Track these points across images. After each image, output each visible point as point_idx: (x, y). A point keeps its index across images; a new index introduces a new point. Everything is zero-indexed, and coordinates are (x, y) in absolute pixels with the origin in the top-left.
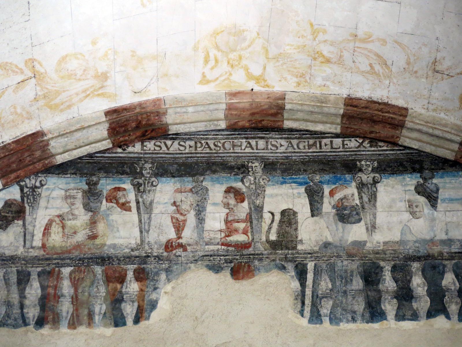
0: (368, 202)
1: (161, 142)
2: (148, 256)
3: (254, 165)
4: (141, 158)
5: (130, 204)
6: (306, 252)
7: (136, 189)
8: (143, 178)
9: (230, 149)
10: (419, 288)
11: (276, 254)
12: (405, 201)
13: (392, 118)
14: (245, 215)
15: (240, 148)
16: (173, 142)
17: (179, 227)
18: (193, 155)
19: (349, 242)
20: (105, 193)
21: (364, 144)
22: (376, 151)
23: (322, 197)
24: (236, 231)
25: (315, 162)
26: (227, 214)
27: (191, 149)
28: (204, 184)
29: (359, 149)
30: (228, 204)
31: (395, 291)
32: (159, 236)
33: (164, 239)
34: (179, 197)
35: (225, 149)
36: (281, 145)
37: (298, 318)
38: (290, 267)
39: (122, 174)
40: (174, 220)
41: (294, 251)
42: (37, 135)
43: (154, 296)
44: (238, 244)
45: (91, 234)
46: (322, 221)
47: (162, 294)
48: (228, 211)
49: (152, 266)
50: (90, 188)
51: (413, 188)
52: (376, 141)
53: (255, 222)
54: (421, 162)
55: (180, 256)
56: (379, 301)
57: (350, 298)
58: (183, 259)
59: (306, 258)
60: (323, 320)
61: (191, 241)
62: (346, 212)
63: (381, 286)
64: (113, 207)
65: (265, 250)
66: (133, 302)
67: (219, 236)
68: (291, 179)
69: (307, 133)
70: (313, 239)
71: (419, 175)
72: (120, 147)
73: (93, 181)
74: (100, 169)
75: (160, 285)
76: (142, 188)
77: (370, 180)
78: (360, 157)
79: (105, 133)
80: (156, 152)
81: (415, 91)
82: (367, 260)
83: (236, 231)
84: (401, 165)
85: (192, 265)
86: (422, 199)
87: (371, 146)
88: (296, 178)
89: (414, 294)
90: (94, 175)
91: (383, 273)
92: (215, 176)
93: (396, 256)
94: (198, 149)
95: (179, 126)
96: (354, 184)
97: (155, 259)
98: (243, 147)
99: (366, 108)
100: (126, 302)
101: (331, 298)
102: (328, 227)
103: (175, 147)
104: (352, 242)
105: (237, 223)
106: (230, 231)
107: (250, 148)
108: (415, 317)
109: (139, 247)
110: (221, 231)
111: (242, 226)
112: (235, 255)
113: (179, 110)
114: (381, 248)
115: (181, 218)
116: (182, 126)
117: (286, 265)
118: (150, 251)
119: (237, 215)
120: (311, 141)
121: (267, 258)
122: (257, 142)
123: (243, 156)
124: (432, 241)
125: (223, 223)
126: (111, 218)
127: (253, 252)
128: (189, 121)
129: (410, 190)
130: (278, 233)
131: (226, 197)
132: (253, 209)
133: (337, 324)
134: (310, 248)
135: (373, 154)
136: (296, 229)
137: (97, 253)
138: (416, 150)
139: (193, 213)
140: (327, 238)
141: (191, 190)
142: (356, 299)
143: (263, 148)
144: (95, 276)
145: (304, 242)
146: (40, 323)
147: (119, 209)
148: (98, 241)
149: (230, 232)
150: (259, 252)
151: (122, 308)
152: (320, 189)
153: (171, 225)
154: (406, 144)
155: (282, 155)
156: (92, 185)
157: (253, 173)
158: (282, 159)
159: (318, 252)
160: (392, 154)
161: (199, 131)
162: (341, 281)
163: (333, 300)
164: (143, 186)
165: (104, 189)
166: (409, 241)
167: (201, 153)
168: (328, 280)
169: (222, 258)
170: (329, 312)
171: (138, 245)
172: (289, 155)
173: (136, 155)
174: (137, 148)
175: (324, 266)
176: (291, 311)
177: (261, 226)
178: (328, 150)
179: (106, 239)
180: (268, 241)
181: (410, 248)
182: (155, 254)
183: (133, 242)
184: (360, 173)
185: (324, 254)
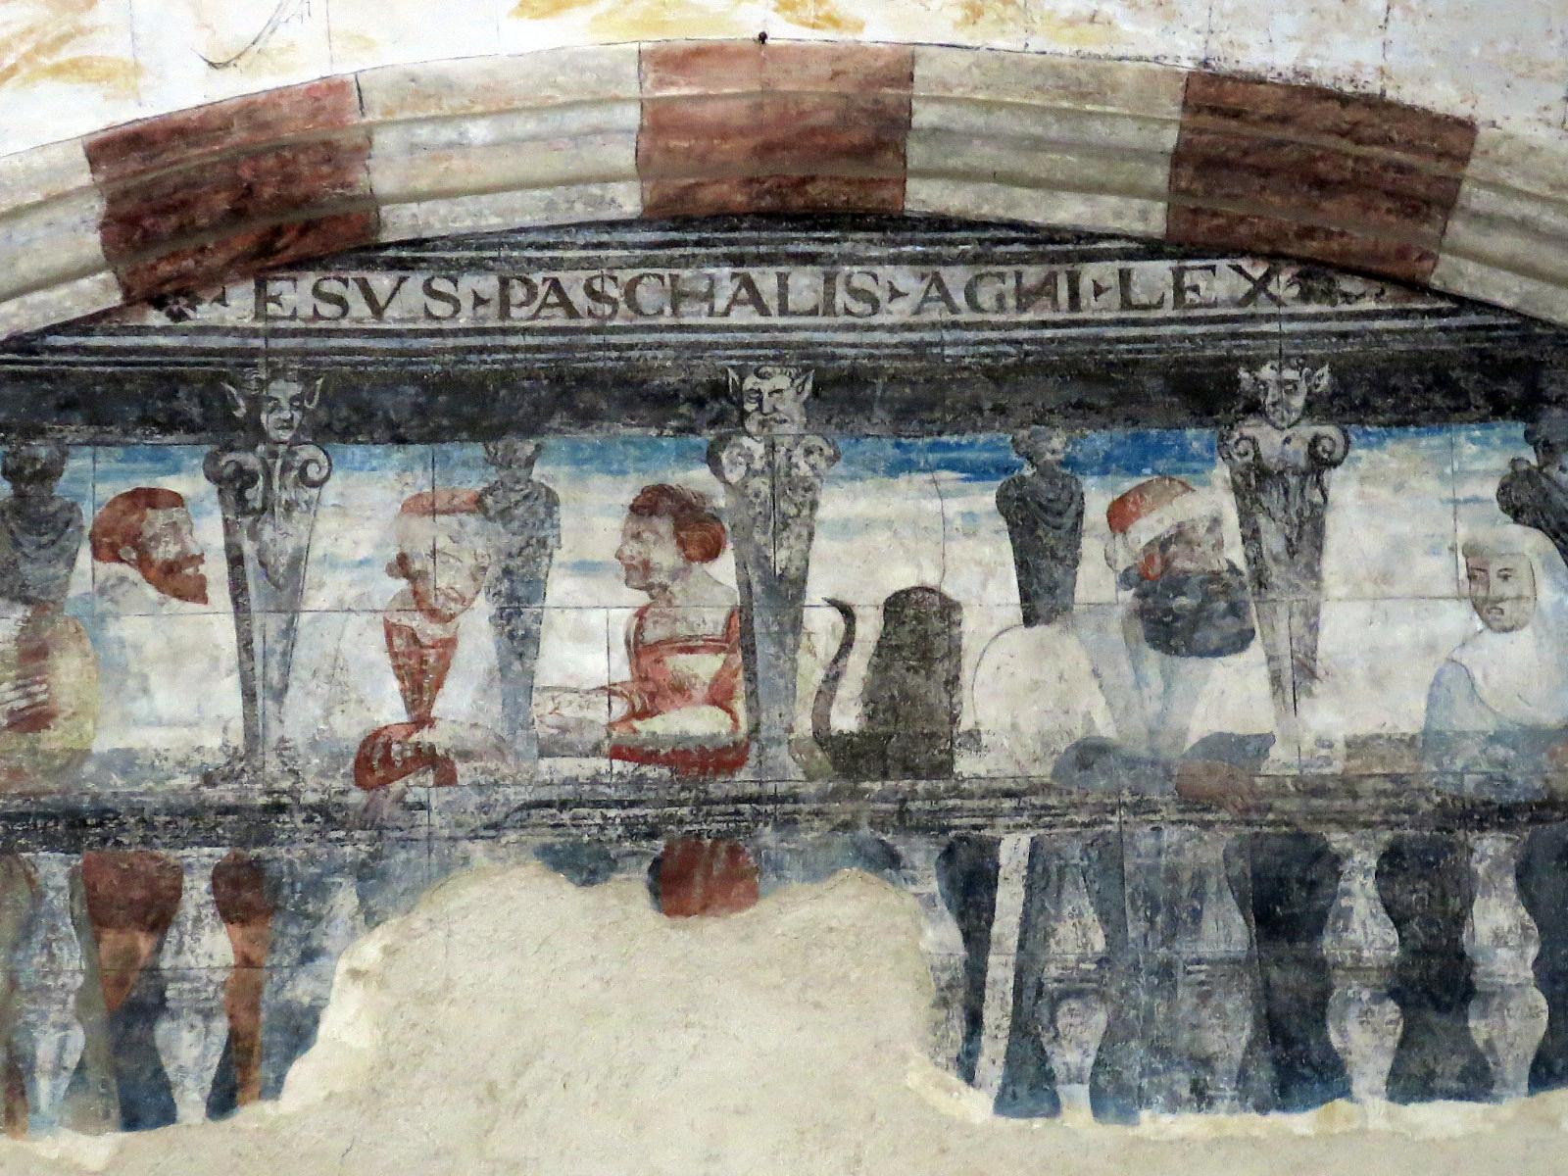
0: (1284, 557)
1: (345, 282)
2: (280, 808)
3: (766, 386)
4: (254, 352)
5: (202, 569)
6: (995, 785)
7: (231, 498)
8: (261, 448)
9: (661, 312)
10: (1502, 953)
11: (856, 795)
12: (1453, 549)
13: (1400, 169)
14: (721, 617)
15: (706, 307)
16: (402, 280)
18: (488, 341)
19: (1193, 739)
20: (88, 515)
21: (1272, 288)
22: (1325, 317)
23: (1076, 530)
24: (681, 689)
25: (1045, 368)
26: (641, 615)
27: (481, 310)
28: (538, 472)
29: (1250, 309)
30: (646, 567)
31: (1390, 967)
32: (328, 713)
33: (349, 729)
34: (424, 533)
35: (639, 312)
36: (895, 294)
37: (949, 1090)
38: (918, 859)
39: (167, 428)
40: (397, 642)
41: (942, 785)
43: (301, 990)
44: (686, 752)
45: (23, 703)
46: (1071, 642)
47: (337, 979)
48: (641, 598)
49: (298, 853)
50: (20, 495)
51: (1490, 490)
52: (1330, 273)
53: (765, 649)
54: (1529, 371)
55: (422, 806)
56: (1317, 1010)
57: (1186, 997)
58: (436, 820)
59: (992, 815)
60: (1063, 1099)
61: (474, 739)
62: (1183, 601)
63: (1328, 945)
64: (122, 579)
65: (810, 778)
66: (208, 1015)
67: (599, 714)
68: (934, 447)
69: (1013, 234)
70: (1029, 725)
71: (1518, 429)
72: (159, 303)
73: (35, 459)
74: (67, 406)
75: (332, 937)
76: (256, 495)
77: (1297, 454)
78: (1252, 348)
79: (91, 244)
80: (322, 324)
81: (1504, 46)
82: (1271, 824)
83: (681, 689)
84: (1442, 381)
85: (478, 850)
87: (1305, 296)
88: (959, 446)
89: (1479, 977)
90: (42, 432)
91: (1342, 884)
92: (591, 437)
93: (1403, 802)
94: (514, 312)
95: (424, 206)
96: (1221, 472)
97: (309, 820)
98: (721, 304)
99: (1284, 120)
100: (174, 1016)
101: (1103, 998)
102: (1096, 673)
104: (1204, 741)
105: (683, 656)
107: (751, 308)
109: (239, 766)
110: (610, 690)
111: (705, 667)
112: (671, 803)
113: (424, 133)
114: (1338, 767)
115: (431, 631)
116: (442, 207)
117: (900, 848)
118: (286, 784)
119: (685, 619)
120: (1033, 275)
121: (817, 813)
122: (783, 279)
123: (715, 345)
125: (620, 652)
126: (113, 630)
127: (753, 789)
128: (473, 181)
129: (1476, 500)
130: (871, 699)
131: (637, 536)
132: (757, 589)
133: (1126, 1116)
134: (1011, 769)
135: (1313, 334)
136: (953, 682)
137: (51, 793)
138: (1511, 312)
139: (483, 609)
140: (1091, 722)
141: (479, 501)
142: (1213, 1002)
143: (809, 306)
144: (38, 896)
145: (985, 739)
147: (151, 592)
148: (53, 739)
149: (652, 696)
150: (782, 788)
151: (159, 1043)
152: (1065, 496)
153: (386, 661)
154: (1464, 288)
155: (896, 338)
157: (763, 424)
158: (898, 357)
159: (1046, 788)
160: (1402, 332)
161: (522, 230)
162: (1151, 921)
163: (1111, 1008)
164: (260, 483)
165: (83, 497)
166: (1464, 734)
167: (526, 331)
168: (1090, 916)
169: (612, 813)
170: (1090, 1061)
171: (234, 756)
172: (928, 336)
173: (230, 342)
174: (238, 306)
175: (1074, 852)
176: (918, 1057)
177: (795, 670)
178: (1106, 316)
179: (89, 726)
180: (823, 737)
181: (1466, 769)
182: (311, 798)
183: (213, 741)
184: (1252, 421)
185: (1075, 797)
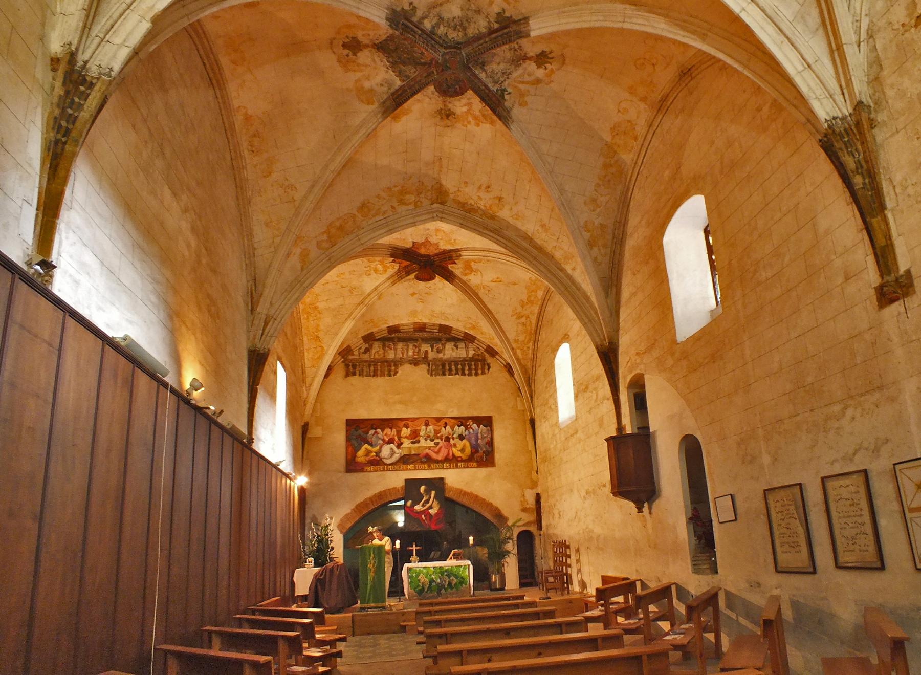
17: (403, 354)
42: (373, 332)
103: (401, 335)
106: (414, 355)
108: (452, 375)
124: (456, 358)
146: (374, 376)
174: (393, 335)
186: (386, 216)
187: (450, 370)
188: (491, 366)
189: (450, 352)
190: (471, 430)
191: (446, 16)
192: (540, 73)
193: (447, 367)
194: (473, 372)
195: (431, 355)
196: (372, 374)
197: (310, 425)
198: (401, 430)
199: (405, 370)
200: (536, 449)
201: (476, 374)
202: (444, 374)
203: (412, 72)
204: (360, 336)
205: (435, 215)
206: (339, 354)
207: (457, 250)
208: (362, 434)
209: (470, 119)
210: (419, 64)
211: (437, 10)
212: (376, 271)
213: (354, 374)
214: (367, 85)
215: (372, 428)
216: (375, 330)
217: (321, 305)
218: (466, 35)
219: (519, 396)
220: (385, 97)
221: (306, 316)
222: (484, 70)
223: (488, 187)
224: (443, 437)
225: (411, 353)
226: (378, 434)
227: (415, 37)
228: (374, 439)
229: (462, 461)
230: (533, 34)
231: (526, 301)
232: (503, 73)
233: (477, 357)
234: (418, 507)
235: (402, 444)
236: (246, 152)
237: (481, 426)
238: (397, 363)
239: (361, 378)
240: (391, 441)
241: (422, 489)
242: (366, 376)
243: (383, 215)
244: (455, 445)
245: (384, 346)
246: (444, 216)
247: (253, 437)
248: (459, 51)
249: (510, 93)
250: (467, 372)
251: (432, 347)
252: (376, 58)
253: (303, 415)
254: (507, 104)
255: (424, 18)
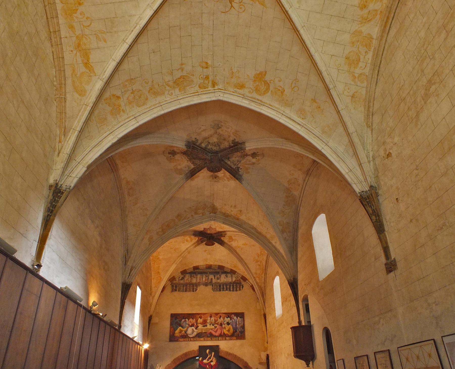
42: (185, 270)
86: (226, 277)
103: (200, 270)
108: (224, 291)
146: (185, 291)
156: (191, 275)
174: (196, 271)
186: (189, 219)
187: (223, 288)
188: (244, 286)
189: (223, 279)
190: (233, 320)
191: (211, 142)
192: (254, 160)
193: (222, 287)
194: (235, 289)
195: (214, 281)
196: (184, 290)
197: (152, 316)
198: (198, 320)
199: (201, 288)
200: (267, 330)
201: (236, 290)
202: (220, 291)
203: (198, 162)
204: (179, 271)
205: (211, 218)
206: (169, 280)
207: (225, 232)
208: (178, 321)
209: (225, 178)
210: (201, 159)
211: (207, 140)
212: (187, 241)
213: (176, 290)
214: (179, 167)
215: (183, 319)
216: (187, 268)
217: (161, 257)
218: (220, 148)
219: (258, 302)
220: (187, 172)
221: (153, 262)
222: (229, 161)
223: (235, 206)
224: (219, 323)
225: (204, 280)
226: (186, 321)
227: (198, 151)
228: (184, 324)
229: (228, 336)
230: (247, 149)
231: (259, 254)
232: (238, 161)
233: (236, 282)
234: (205, 361)
235: (198, 327)
236: (126, 195)
237: (239, 318)
238: (197, 285)
239: (179, 292)
240: (193, 325)
241: (208, 351)
242: (182, 291)
243: (187, 219)
244: (225, 328)
245: (191, 276)
246: (216, 219)
247: (122, 325)
248: (217, 155)
249: (241, 169)
250: (231, 289)
251: (215, 276)
252: (183, 157)
253: (149, 311)
254: (240, 173)
255: (201, 143)
